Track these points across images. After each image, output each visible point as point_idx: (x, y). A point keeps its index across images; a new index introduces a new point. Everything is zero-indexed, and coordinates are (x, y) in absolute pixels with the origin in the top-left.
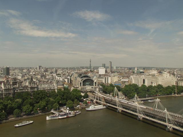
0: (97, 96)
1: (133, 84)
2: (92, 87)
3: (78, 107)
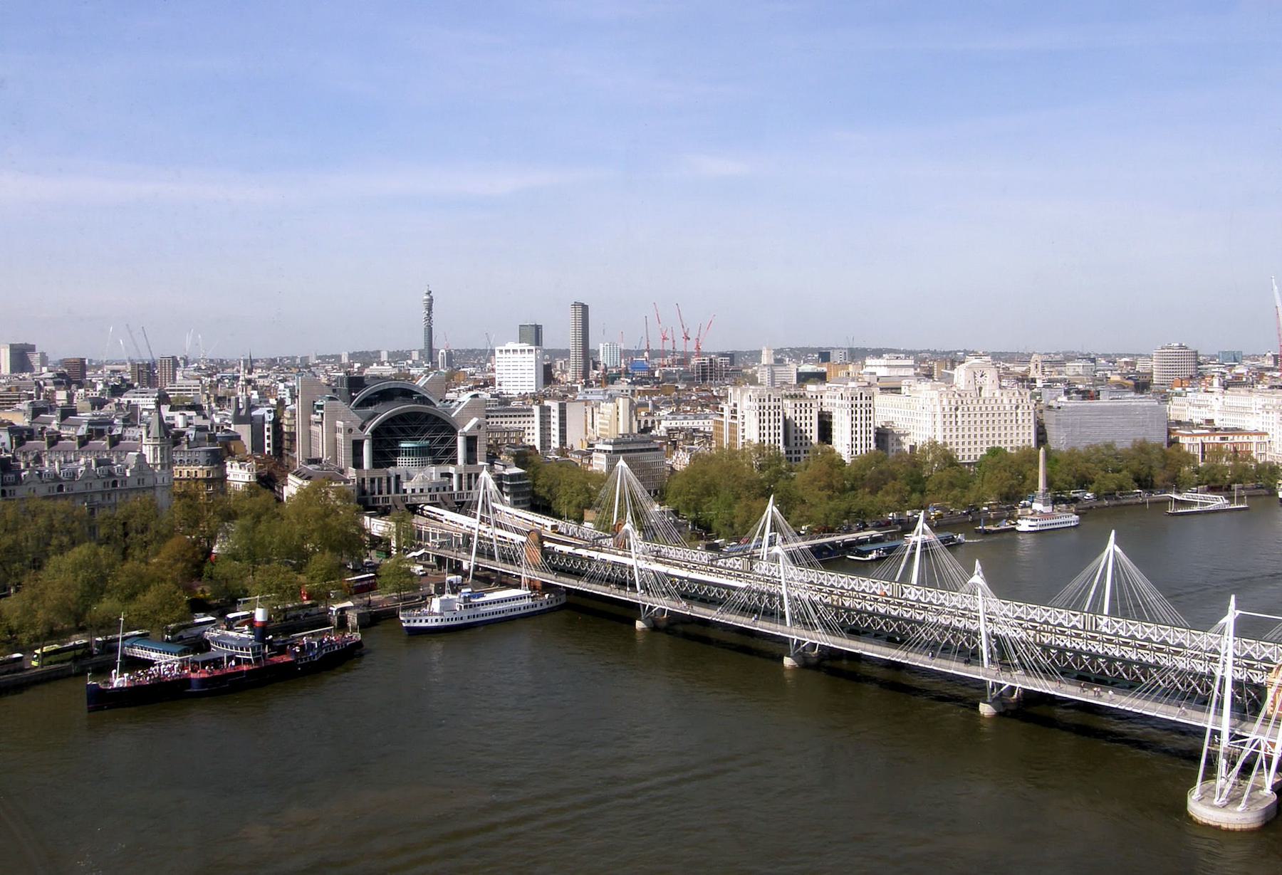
2: (450, 475)
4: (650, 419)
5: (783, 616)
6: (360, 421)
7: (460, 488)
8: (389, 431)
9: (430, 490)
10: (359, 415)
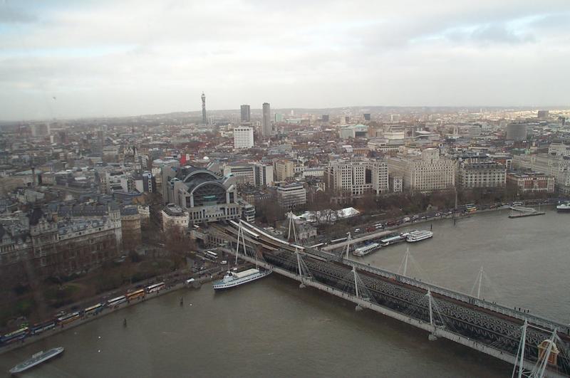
0: (241, 239)
2: (223, 209)
3: (190, 282)
6: (188, 188)
7: (228, 214)
8: (200, 193)
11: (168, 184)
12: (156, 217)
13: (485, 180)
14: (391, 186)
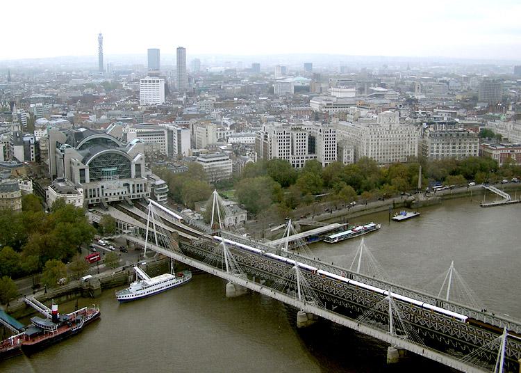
1: (275, 158)
2: (128, 185)
4: (222, 132)
5: (297, 291)
6: (82, 158)
7: (134, 192)
8: (99, 164)
9: (118, 193)
10: (81, 154)
11: (56, 152)
12: (39, 191)
13: (454, 148)
14: (340, 157)
